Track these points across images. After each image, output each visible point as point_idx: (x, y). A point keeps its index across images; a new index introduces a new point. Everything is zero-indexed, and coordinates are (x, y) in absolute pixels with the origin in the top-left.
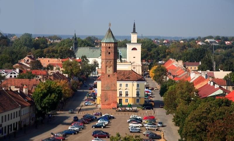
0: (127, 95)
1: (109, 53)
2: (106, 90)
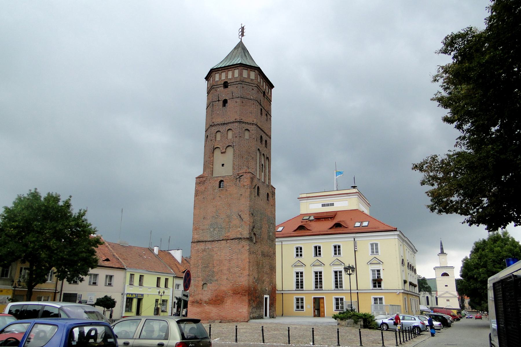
1: (225, 102)
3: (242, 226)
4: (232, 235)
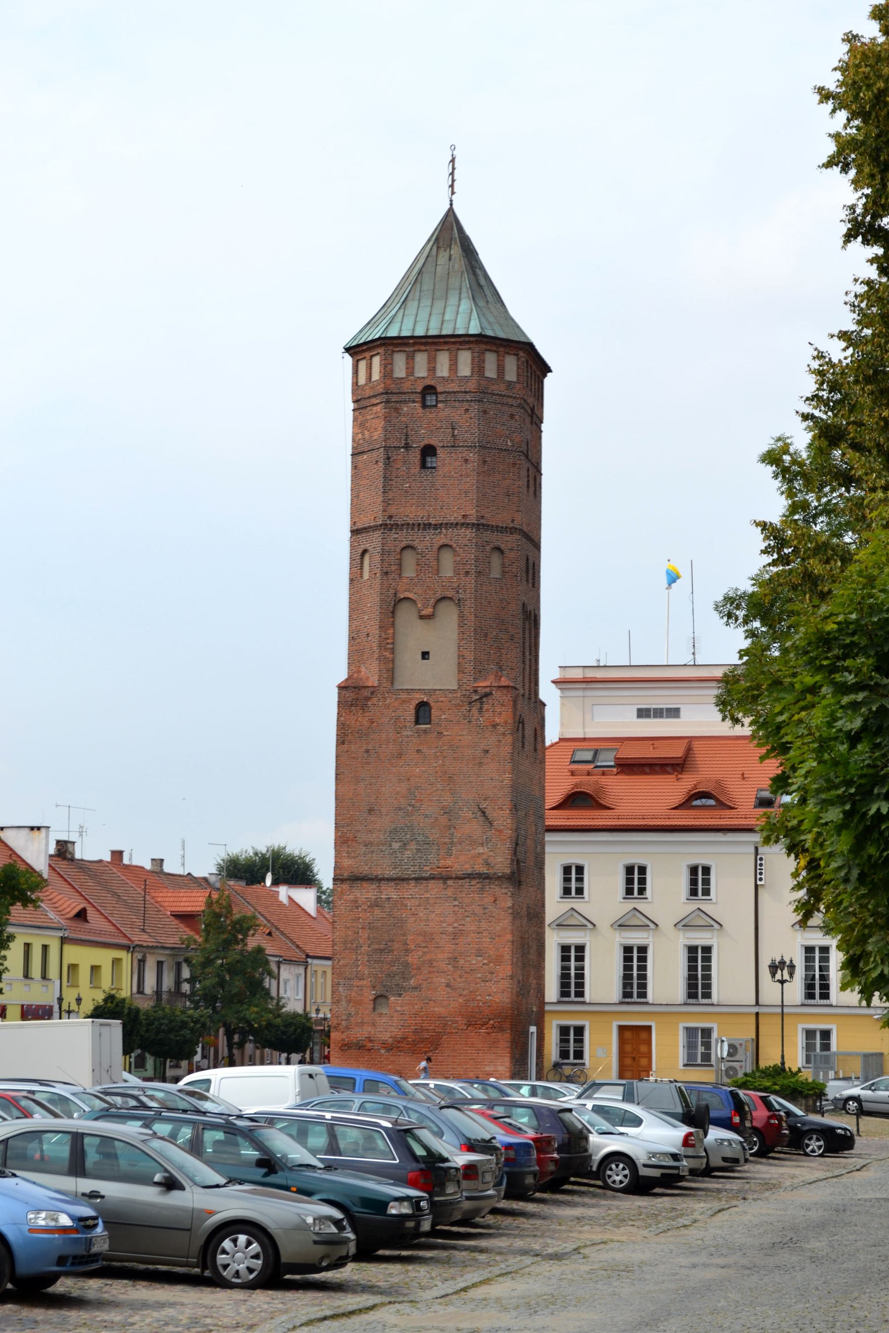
0: (698, 984)
1: (429, 451)
2: (390, 873)
3: (488, 840)
4: (460, 863)
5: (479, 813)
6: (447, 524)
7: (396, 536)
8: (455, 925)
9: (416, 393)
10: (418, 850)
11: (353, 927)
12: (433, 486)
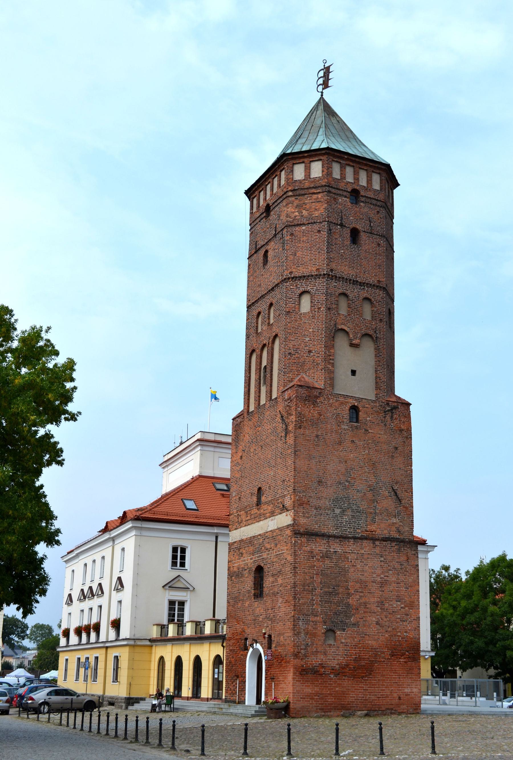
3: (399, 514)
5: (393, 493)
6: (367, 284)
7: (336, 284)
8: (382, 576)
9: (347, 191)
10: (353, 516)
11: (309, 573)
12: (359, 256)
